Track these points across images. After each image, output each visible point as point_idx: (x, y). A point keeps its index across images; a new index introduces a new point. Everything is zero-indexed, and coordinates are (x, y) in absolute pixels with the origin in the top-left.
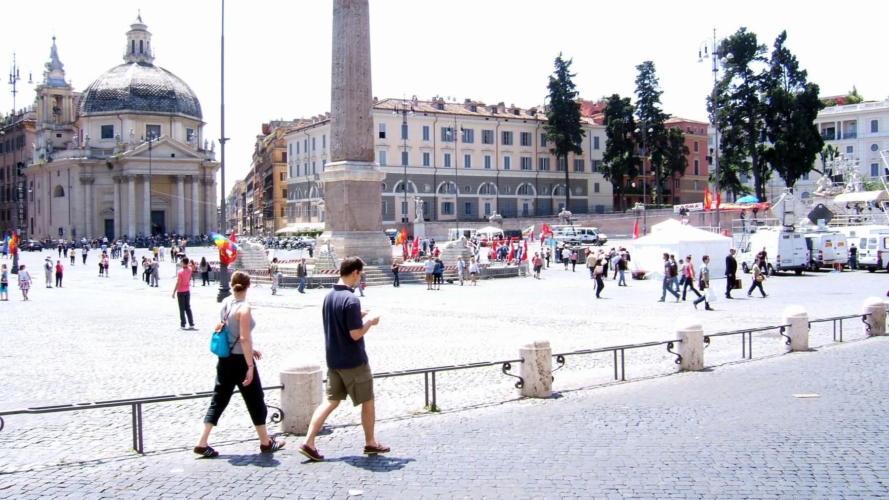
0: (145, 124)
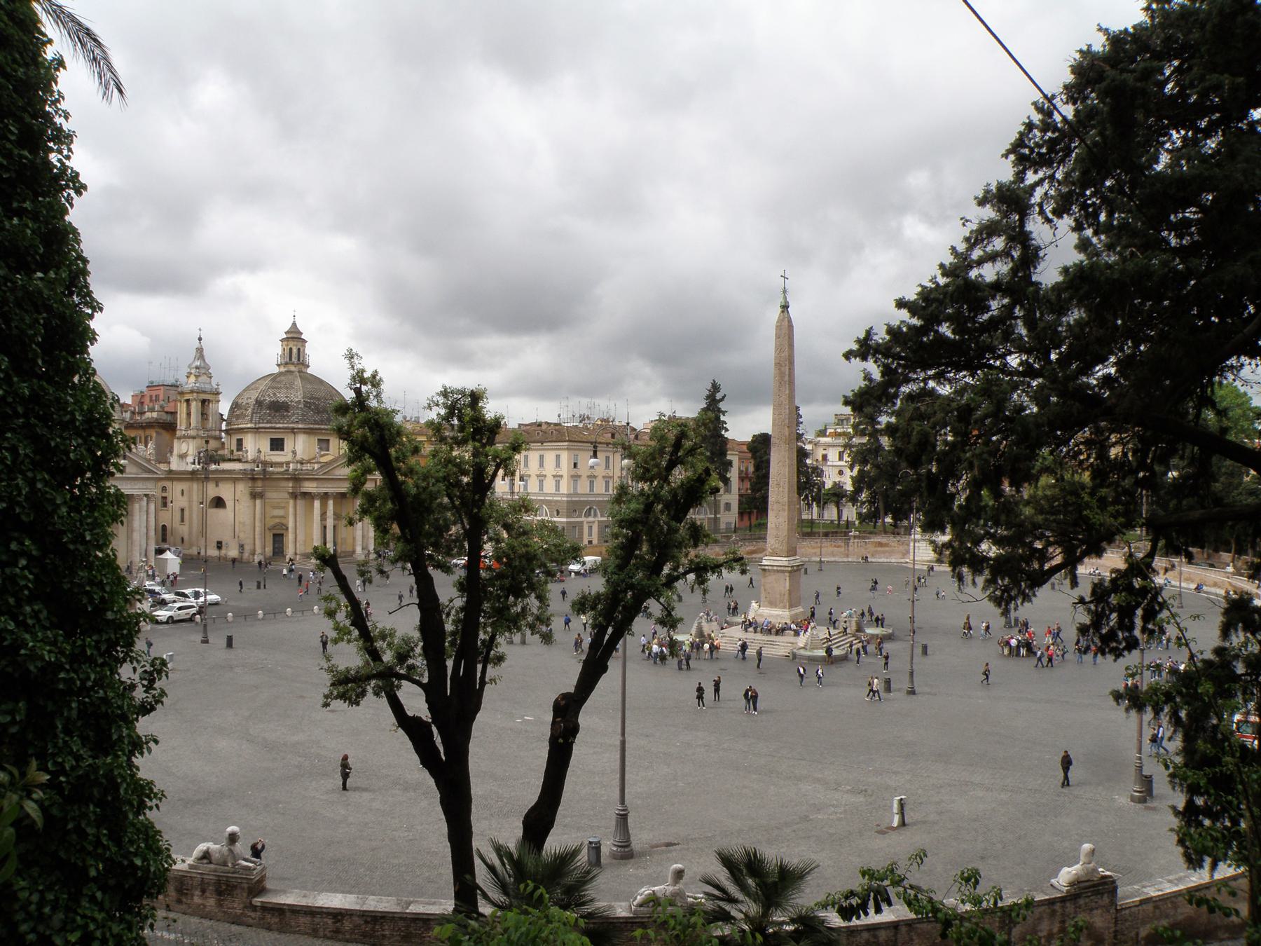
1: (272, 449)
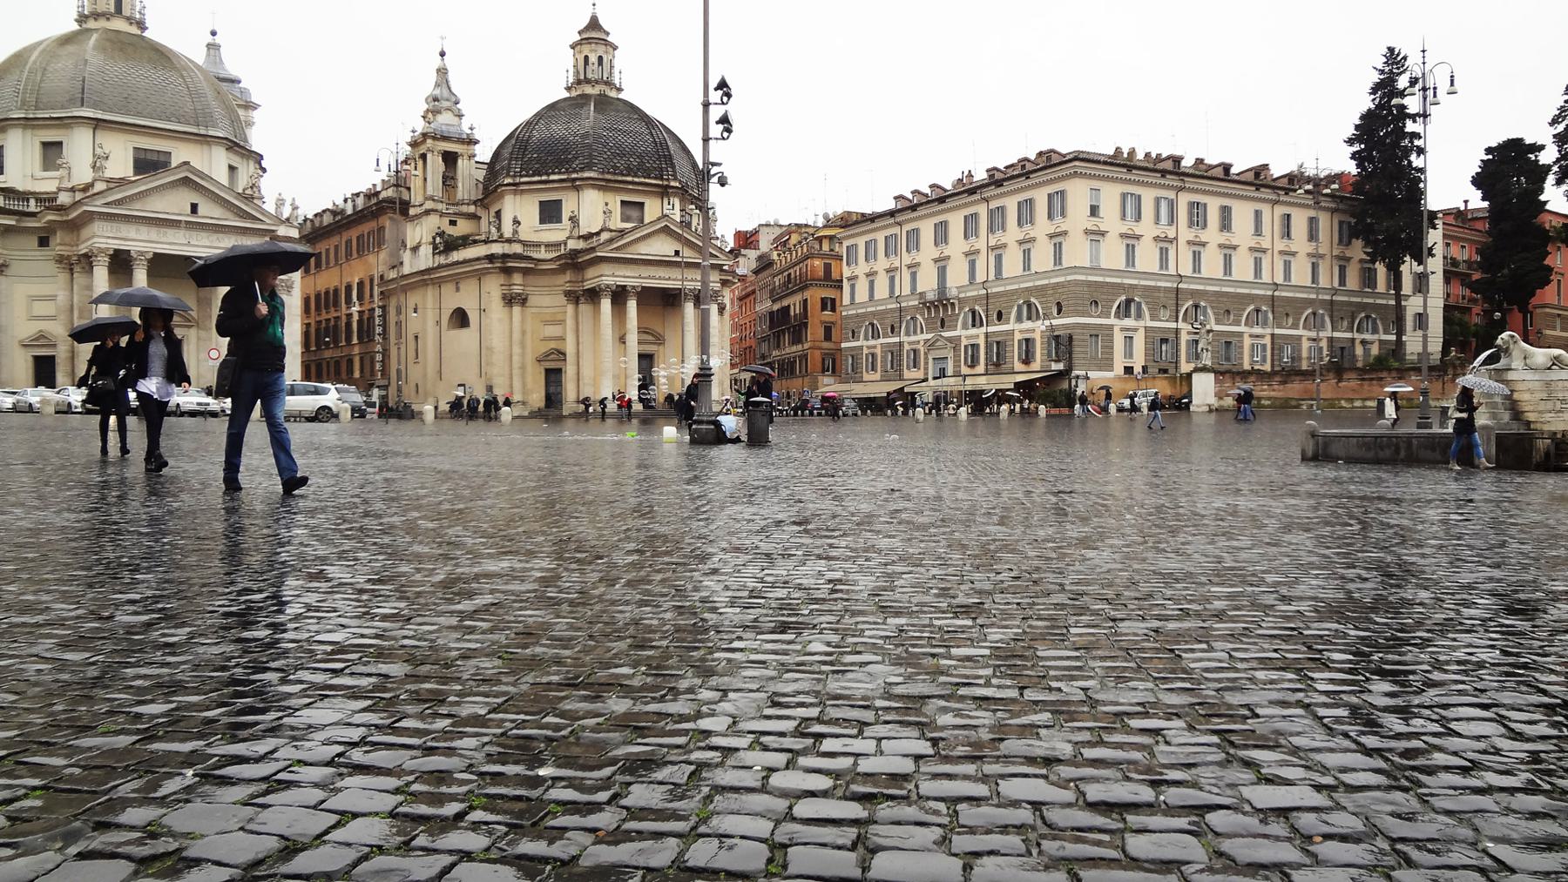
0: (619, 199)
1: (542, 221)
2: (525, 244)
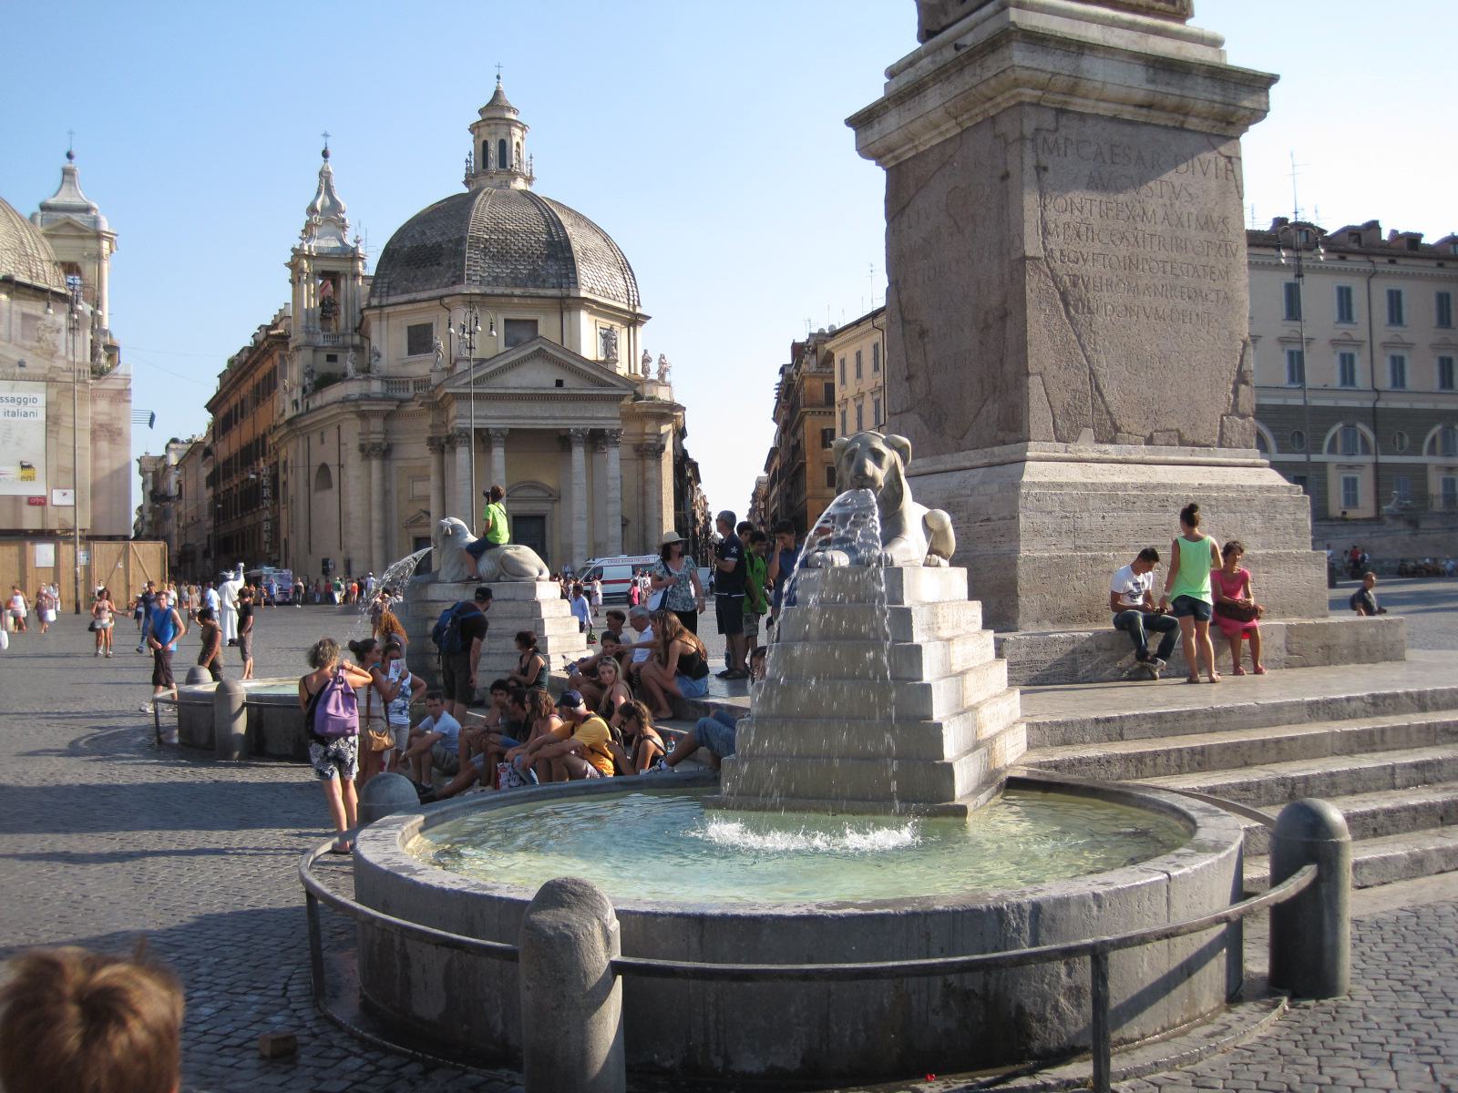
1: (409, 354)
2: (387, 380)
